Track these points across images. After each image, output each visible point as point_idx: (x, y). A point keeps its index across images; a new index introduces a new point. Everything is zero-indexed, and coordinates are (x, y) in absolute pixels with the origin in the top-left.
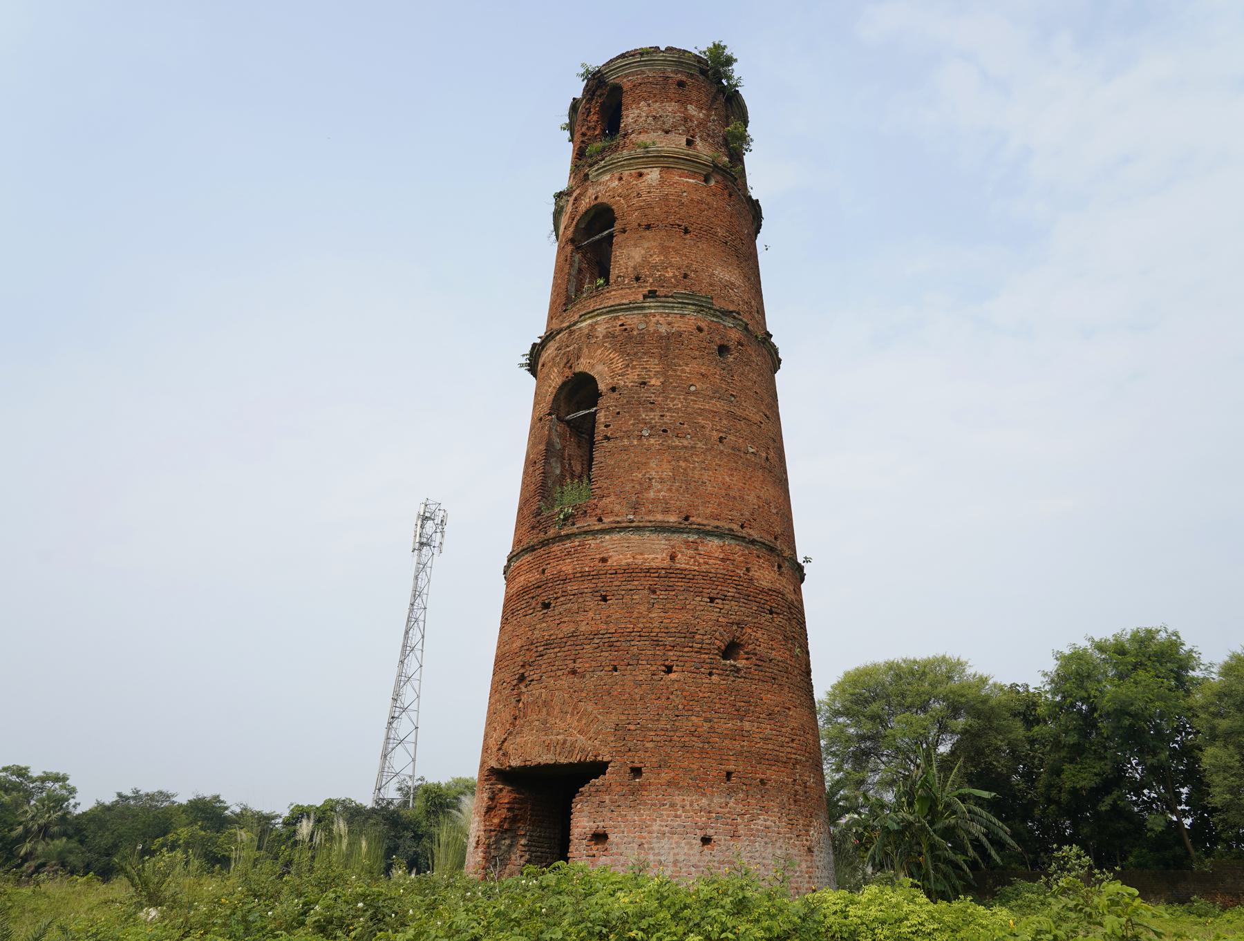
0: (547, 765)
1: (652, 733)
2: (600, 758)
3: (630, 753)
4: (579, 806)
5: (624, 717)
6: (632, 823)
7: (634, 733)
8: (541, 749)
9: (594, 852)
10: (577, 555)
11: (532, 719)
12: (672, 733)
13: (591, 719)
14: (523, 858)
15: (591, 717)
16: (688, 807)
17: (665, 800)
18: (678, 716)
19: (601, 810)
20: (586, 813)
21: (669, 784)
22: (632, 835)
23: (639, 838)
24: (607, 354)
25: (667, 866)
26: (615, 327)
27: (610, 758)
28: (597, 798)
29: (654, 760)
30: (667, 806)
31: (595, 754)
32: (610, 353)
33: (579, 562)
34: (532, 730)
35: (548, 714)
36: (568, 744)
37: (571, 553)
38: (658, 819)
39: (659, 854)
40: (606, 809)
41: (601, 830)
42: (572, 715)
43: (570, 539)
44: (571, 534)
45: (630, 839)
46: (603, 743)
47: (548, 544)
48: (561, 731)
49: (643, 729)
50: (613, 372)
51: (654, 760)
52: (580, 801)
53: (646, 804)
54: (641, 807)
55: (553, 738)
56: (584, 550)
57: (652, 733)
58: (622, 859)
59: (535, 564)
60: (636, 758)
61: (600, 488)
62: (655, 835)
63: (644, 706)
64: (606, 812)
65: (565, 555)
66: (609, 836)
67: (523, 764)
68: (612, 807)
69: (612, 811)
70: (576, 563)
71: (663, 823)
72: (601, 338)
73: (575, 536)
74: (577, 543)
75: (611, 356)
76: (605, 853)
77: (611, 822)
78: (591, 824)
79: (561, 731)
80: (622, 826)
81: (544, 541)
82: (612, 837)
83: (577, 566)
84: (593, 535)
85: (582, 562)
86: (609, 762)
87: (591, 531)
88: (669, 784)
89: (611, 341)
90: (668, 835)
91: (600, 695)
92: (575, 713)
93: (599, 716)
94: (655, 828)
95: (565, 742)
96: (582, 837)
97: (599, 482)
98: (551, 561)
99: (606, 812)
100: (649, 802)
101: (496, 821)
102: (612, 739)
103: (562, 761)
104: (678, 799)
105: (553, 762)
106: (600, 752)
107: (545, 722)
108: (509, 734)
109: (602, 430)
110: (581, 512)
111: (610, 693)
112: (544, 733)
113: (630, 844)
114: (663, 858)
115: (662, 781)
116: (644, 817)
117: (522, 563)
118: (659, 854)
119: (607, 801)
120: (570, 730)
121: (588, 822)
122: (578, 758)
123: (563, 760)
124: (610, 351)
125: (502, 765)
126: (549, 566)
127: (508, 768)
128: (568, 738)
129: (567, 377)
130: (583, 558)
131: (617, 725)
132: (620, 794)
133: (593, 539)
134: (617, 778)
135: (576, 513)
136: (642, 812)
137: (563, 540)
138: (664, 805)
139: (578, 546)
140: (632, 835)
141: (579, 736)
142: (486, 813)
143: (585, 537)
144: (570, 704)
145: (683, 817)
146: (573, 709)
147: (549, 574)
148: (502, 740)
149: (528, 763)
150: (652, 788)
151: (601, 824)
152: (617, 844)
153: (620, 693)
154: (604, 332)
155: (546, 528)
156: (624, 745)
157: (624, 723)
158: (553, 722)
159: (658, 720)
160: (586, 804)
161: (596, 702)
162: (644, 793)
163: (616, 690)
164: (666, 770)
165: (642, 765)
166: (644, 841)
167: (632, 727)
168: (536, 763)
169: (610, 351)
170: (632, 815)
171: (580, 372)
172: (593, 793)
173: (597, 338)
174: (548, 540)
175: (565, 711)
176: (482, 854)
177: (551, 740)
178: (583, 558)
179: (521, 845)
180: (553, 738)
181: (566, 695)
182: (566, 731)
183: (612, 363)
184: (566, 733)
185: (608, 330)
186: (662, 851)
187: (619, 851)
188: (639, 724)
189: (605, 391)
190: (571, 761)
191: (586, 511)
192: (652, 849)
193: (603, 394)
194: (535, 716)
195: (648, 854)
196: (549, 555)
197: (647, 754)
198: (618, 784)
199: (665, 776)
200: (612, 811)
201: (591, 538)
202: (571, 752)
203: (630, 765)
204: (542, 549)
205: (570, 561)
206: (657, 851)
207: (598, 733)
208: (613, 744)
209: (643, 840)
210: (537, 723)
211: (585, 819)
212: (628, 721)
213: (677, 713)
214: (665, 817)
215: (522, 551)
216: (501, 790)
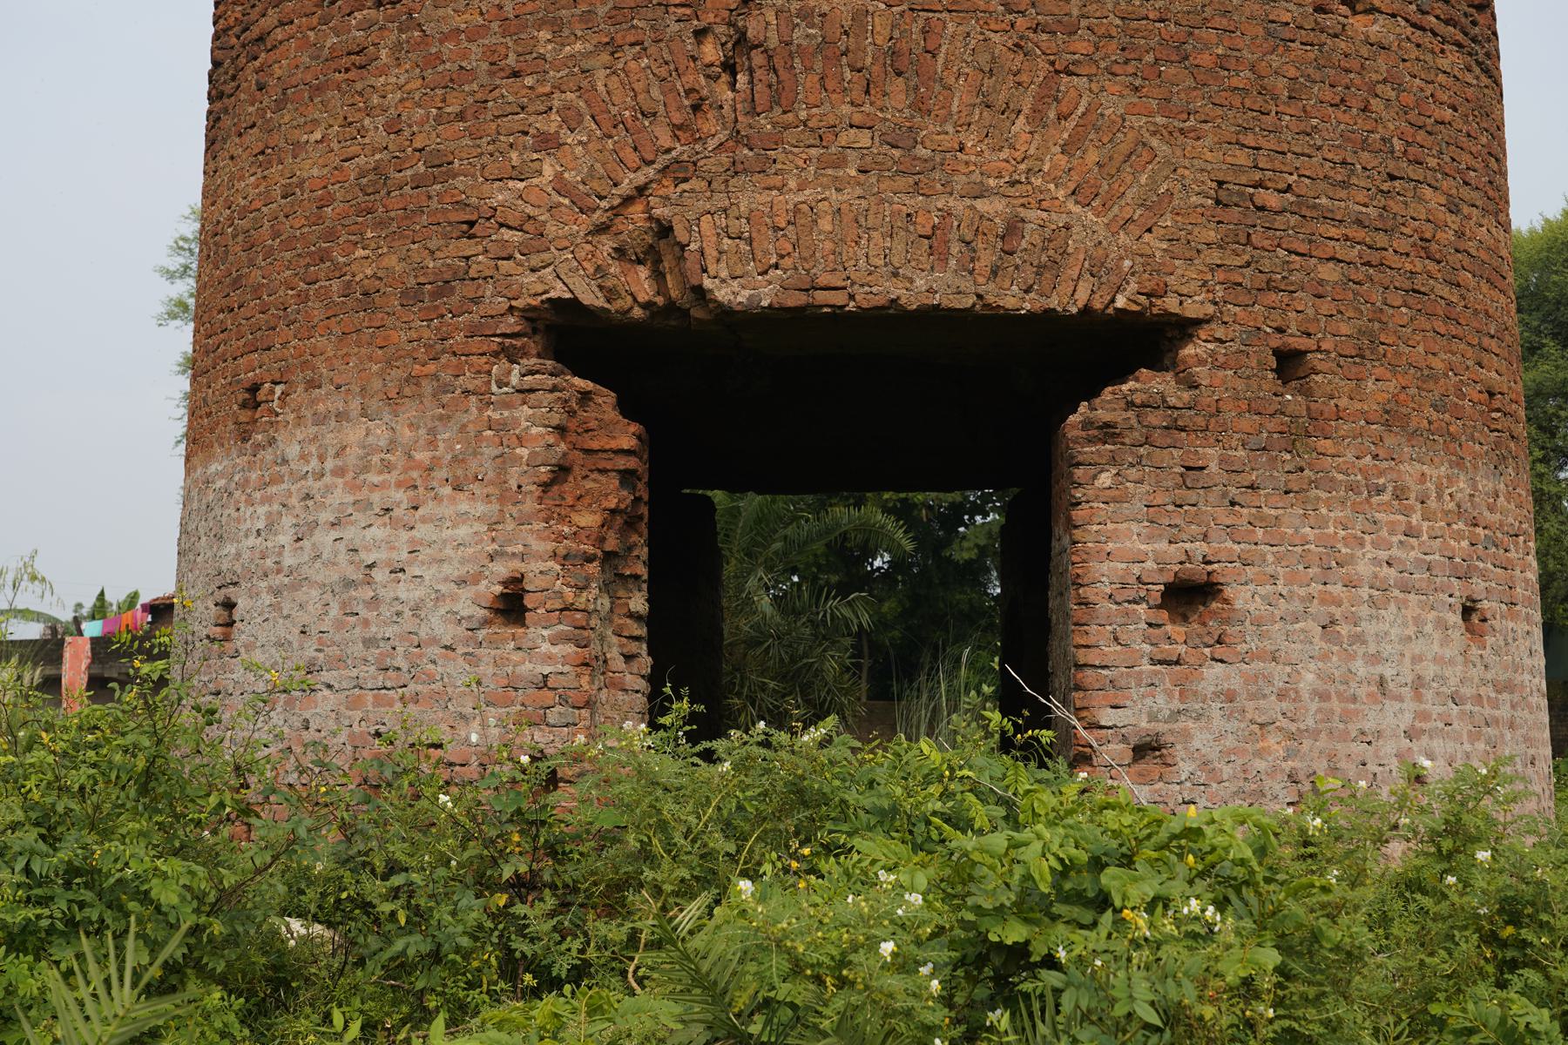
0: (933, 318)
1: (1333, 232)
2: (1171, 304)
3: (1273, 297)
4: (1105, 479)
5: (1242, 158)
6: (1299, 549)
7: (1280, 221)
8: (899, 247)
9: (1182, 649)
11: (831, 120)
12: (1381, 239)
13: (1124, 148)
14: (635, 665)
15: (1125, 142)
16: (1432, 503)
17: (1381, 474)
18: (1392, 177)
19: (1192, 496)
20: (1138, 506)
21: (1392, 418)
22: (1302, 592)
23: (1323, 602)
25: (1400, 699)
27: (1211, 309)
28: (1175, 452)
29: (1345, 329)
30: (1386, 497)
31: (1149, 286)
34: (841, 163)
35: (920, 106)
36: (1031, 235)
38: (1367, 537)
39: (1375, 659)
40: (1213, 496)
41: (1197, 571)
42: (1037, 118)
45: (1297, 606)
46: (1177, 249)
48: (992, 182)
49: (1304, 209)
51: (1345, 329)
52: (1113, 460)
53: (1332, 485)
54: (1324, 495)
55: (958, 206)
57: (1333, 232)
58: (1279, 672)
60: (1292, 315)
62: (1365, 592)
63: (1302, 126)
64: (1212, 508)
66: (1228, 592)
67: (795, 300)
68: (1233, 491)
69: (1233, 504)
71: (1384, 555)
76: (1220, 651)
77: (1229, 544)
78: (1162, 545)
79: (992, 182)
80: (1270, 558)
82: (1242, 596)
86: (1198, 322)
88: (1392, 418)
90: (1396, 593)
91: (1149, 58)
92: (1052, 115)
93: (1155, 142)
94: (1363, 568)
95: (1014, 227)
96: (1131, 594)
99: (1212, 508)
100: (1340, 477)
101: (588, 519)
102: (1212, 236)
103: (1009, 302)
104: (1409, 471)
105: (968, 302)
106: (1171, 280)
107: (901, 138)
108: (664, 170)
111: (1186, 58)
112: (903, 182)
113: (1297, 620)
114: (1389, 672)
115: (1371, 406)
116: (1331, 530)
118: (1375, 659)
119: (1214, 467)
120: (1037, 181)
121: (1150, 539)
122: (1082, 296)
123: (1012, 298)
125: (611, 294)
127: (637, 312)
128: (1032, 214)
131: (1220, 183)
132: (1253, 442)
134: (1240, 385)
136: (1324, 511)
138: (1380, 491)
140: (1302, 592)
141: (1077, 209)
142: (546, 486)
144: (1024, 78)
145: (1425, 537)
146: (1040, 98)
148: (625, 188)
149: (821, 297)
150: (1346, 427)
151: (1199, 548)
152: (1258, 623)
153: (1222, 63)
156: (1248, 264)
157: (1244, 180)
158: (949, 141)
159: (1344, 184)
160: (1133, 473)
161: (1138, 82)
162: (1325, 445)
163: (1207, 46)
164: (1379, 371)
165: (1310, 343)
166: (1338, 612)
167: (1272, 199)
168: (880, 301)
170: (1292, 520)
172: (1157, 434)
175: (1000, 100)
176: (570, 649)
177: (947, 214)
179: (631, 615)
180: (958, 206)
181: (996, 38)
182: (1013, 184)
184: (1011, 191)
186: (1388, 649)
187: (1268, 645)
188: (1289, 189)
190: (1054, 303)
192: (1359, 639)
194: (846, 109)
195: (1352, 657)
197: (1326, 306)
198: (1245, 407)
199: (1378, 389)
200: (1233, 504)
202: (1049, 268)
203: (1276, 341)
206: (1372, 649)
207: (1154, 205)
208: (1215, 257)
209: (1333, 609)
210: (864, 139)
211: (1135, 527)
212: (1257, 176)
213: (1392, 166)
214: (1384, 533)
216: (585, 396)
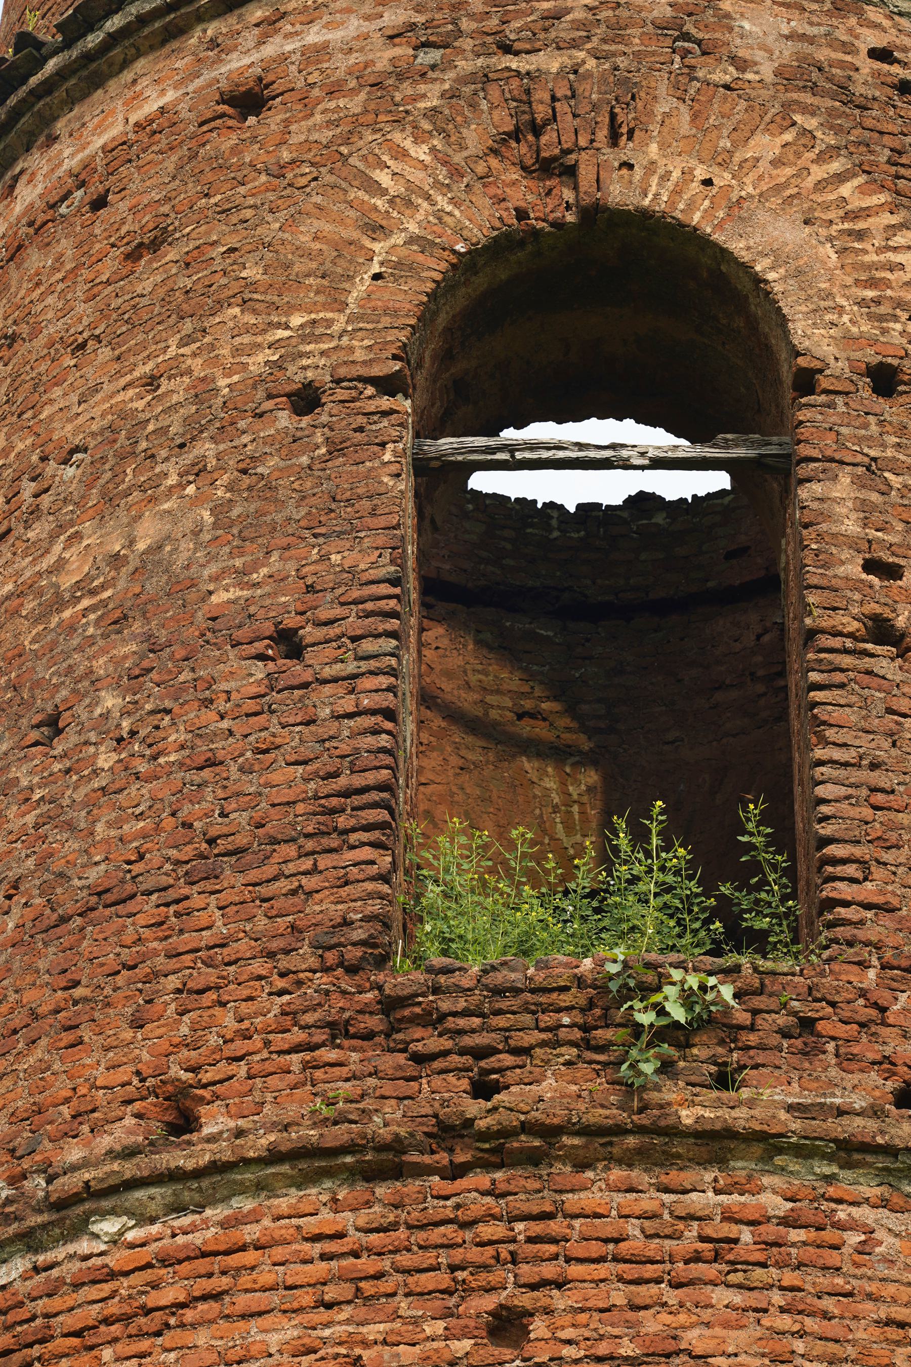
10: (790, 1278)
24: (818, 172)
26: (848, 48)
32: (840, 178)
33: (811, 1324)
37: (739, 1252)
43: (720, 1161)
44: (761, 1137)
47: (534, 1159)
50: (872, 283)
56: (833, 1258)
59: (404, 1259)
61: (890, 909)
65: (697, 1258)
70: (785, 1322)
72: (767, 71)
73: (767, 1158)
74: (779, 1206)
75: (846, 190)
81: (506, 1133)
83: (799, 1346)
84: (886, 1176)
85: (833, 1328)
87: (890, 1151)
89: (830, 112)
97: (878, 873)
98: (576, 1270)
109: (857, 585)
110: (782, 1020)
117: (250, 1232)
124: (836, 166)
126: (560, 1300)
129: (522, 214)
130: (828, 1304)
133: (884, 1203)
135: (742, 1017)
137: (668, 1160)
139: (786, 1222)
143: (829, 1179)
147: (568, 1352)
154: (787, 51)
155: (480, 1053)
169: (836, 166)
171: (645, 215)
173: (742, 65)
174: (550, 1132)
178: (828, 1304)
183: (860, 235)
185: (807, 48)
189: (840, 367)
191: (807, 1024)
193: (825, 384)
196: (555, 1227)
201: (873, 1191)
204: (480, 1179)
205: (737, 1298)
215: (274, 1157)
